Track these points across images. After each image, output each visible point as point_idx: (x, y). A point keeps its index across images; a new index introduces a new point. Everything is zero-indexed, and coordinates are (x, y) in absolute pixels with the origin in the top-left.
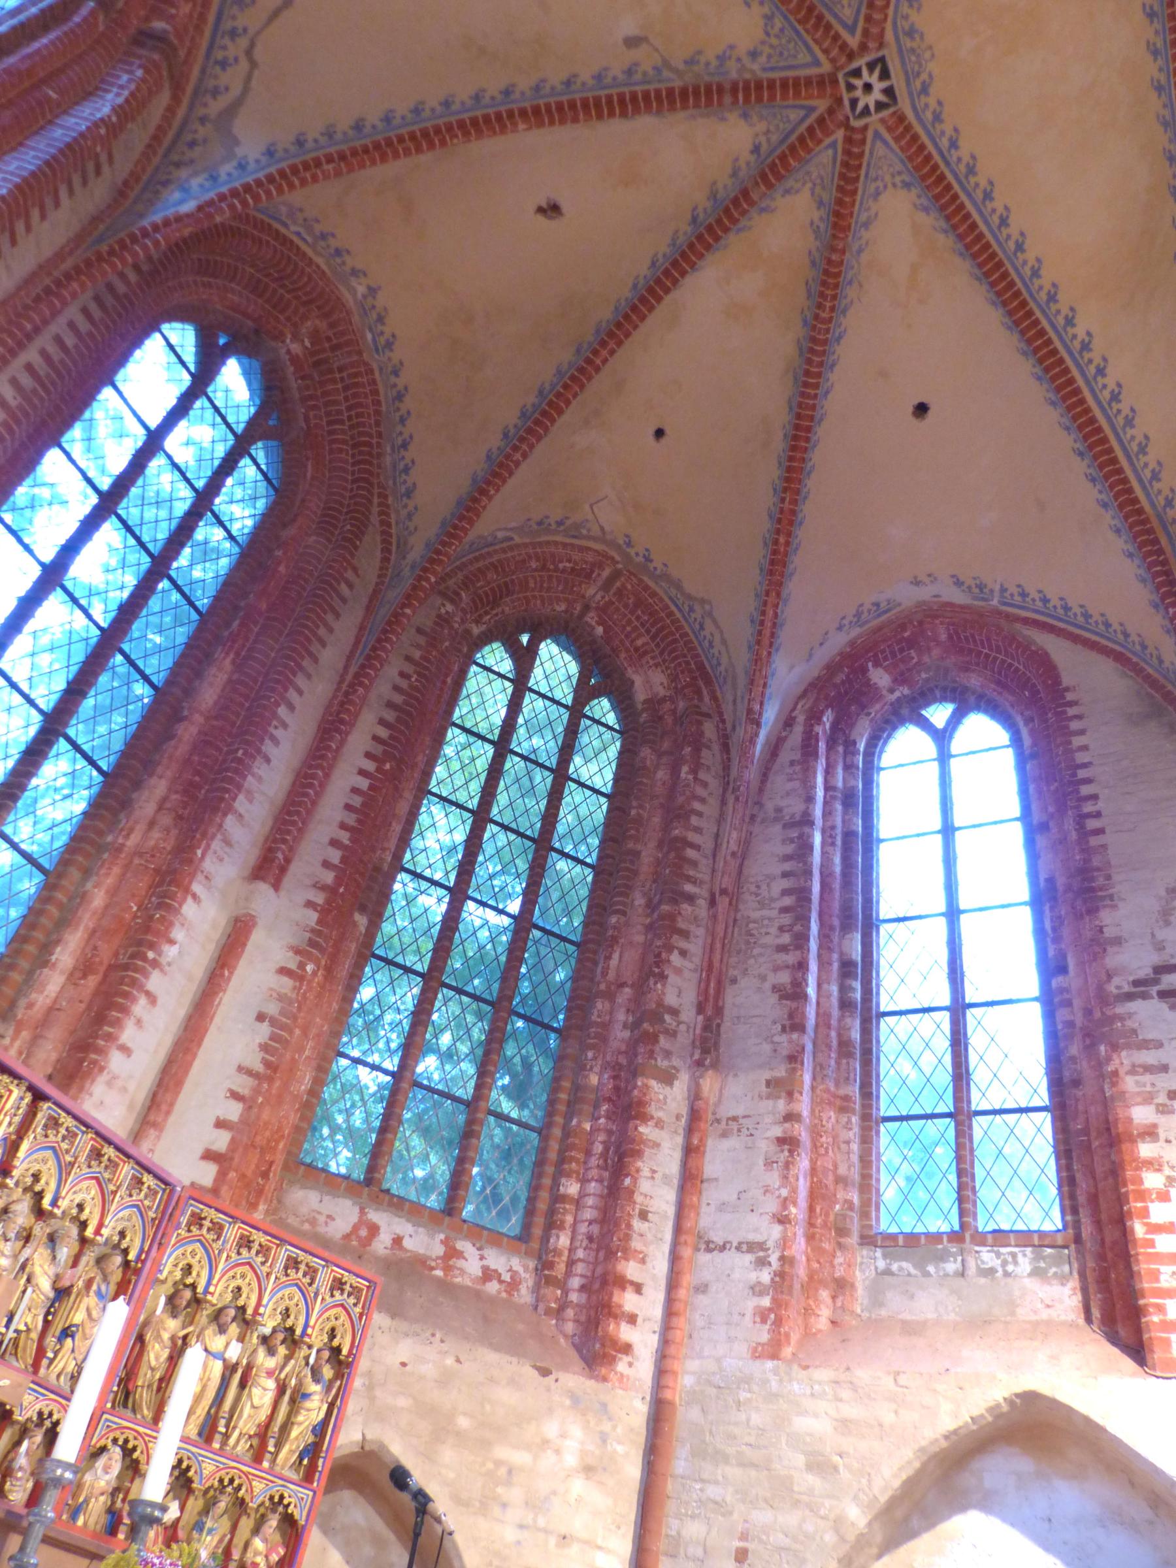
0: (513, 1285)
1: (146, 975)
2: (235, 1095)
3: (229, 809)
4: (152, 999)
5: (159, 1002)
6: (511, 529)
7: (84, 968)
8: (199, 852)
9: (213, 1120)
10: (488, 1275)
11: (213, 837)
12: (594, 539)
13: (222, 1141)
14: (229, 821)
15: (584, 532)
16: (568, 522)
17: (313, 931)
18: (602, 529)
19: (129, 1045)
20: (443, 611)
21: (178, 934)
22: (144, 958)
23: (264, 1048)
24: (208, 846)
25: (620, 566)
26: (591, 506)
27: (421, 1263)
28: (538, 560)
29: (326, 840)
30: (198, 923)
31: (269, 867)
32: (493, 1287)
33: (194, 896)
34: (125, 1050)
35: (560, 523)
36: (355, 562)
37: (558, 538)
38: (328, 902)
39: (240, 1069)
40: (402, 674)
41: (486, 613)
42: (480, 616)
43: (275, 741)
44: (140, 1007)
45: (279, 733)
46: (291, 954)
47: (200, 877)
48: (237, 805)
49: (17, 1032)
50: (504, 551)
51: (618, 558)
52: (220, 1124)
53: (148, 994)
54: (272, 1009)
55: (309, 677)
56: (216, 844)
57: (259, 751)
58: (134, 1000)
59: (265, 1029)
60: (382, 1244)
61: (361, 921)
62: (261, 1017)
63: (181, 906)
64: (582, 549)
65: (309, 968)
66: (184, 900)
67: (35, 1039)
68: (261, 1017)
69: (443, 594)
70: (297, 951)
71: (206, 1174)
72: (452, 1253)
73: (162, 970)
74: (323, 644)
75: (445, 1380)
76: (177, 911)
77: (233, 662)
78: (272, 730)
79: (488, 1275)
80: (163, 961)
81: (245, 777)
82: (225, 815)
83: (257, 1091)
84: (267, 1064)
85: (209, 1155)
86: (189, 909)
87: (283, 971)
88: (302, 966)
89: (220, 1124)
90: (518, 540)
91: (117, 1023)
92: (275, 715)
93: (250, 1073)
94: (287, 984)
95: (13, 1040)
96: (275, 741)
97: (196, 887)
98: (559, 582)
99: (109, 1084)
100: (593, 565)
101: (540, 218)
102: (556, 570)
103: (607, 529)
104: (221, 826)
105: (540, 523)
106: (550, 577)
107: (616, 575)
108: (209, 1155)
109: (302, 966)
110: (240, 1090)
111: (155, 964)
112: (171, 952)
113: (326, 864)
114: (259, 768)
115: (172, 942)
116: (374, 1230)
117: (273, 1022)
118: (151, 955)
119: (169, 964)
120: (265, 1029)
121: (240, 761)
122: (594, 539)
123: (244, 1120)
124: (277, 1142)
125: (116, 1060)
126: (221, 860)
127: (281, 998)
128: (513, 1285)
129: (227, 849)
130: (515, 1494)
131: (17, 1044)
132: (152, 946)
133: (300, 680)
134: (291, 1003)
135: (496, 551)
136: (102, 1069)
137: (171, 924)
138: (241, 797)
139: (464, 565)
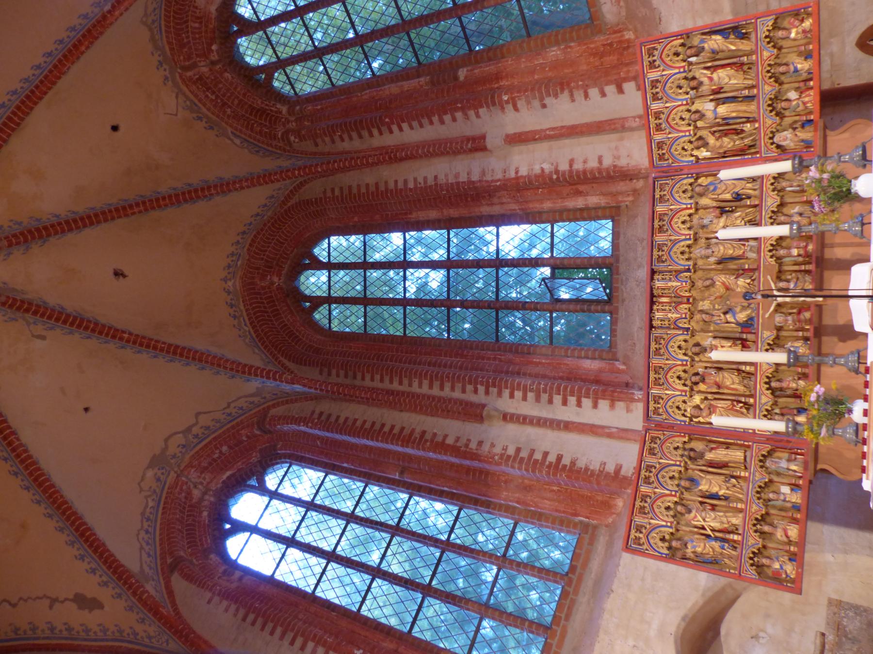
1: (564, 173)
2: (586, 96)
4: (571, 162)
5: (570, 157)
6: (229, 139)
7: (579, 193)
8: (498, 184)
9: (604, 99)
11: (487, 181)
12: (184, 94)
13: (610, 89)
14: (475, 178)
15: (188, 103)
16: (195, 115)
17: (488, 107)
18: (177, 97)
19: (597, 160)
20: (297, 140)
21: (537, 170)
22: (558, 178)
23: (556, 96)
24: (492, 181)
25: (179, 70)
26: (176, 115)
28: (225, 112)
29: (443, 127)
30: (527, 162)
31: (477, 145)
33: (517, 173)
34: (600, 159)
35: (200, 119)
36: (322, 196)
37: (204, 110)
38: (469, 108)
39: (573, 101)
41: (271, 110)
42: (276, 112)
43: (425, 179)
44: (578, 166)
45: (420, 180)
46: (506, 110)
47: (507, 176)
48: (466, 180)
49: (622, 202)
50: (241, 131)
51: (177, 75)
52: (603, 94)
53: (571, 166)
54: (536, 103)
55: (386, 183)
56: (488, 178)
57: (436, 184)
58: (578, 171)
59: (547, 101)
61: (462, 74)
62: (544, 106)
63: (525, 177)
64: (196, 96)
65: (505, 98)
66: (522, 176)
67: (621, 193)
68: (544, 106)
70: (503, 108)
71: (629, 87)
73: (557, 166)
74: (367, 185)
76: (529, 176)
77: (411, 213)
78: (422, 185)
80: (553, 168)
81: (452, 184)
82: (474, 182)
83: (578, 87)
84: (562, 90)
86: (523, 172)
87: (516, 109)
88: (507, 102)
89: (603, 94)
90: (229, 130)
91: (592, 171)
92: (416, 188)
93: (572, 95)
94: (520, 104)
95: (625, 201)
96: (425, 179)
97: (513, 175)
98: (220, 89)
99: (618, 158)
100: (194, 83)
101: (126, 273)
102: (217, 97)
103: (174, 95)
104: (480, 181)
105: (211, 128)
106: (224, 95)
107: (186, 69)
109: (507, 102)
110: (583, 95)
111: (557, 172)
112: (547, 167)
113: (454, 119)
114: (442, 179)
115: (543, 170)
117: (542, 99)
118: (555, 177)
119: (552, 164)
120: (547, 101)
121: (447, 190)
122: (184, 94)
123: (595, 85)
124: (592, 49)
125: (607, 162)
126: (493, 170)
127: (528, 103)
129: (486, 170)
131: (625, 199)
132: (551, 179)
133: (391, 185)
134: (527, 97)
135: (245, 134)
136: (615, 166)
137: (536, 176)
138: (461, 180)
139: (268, 145)
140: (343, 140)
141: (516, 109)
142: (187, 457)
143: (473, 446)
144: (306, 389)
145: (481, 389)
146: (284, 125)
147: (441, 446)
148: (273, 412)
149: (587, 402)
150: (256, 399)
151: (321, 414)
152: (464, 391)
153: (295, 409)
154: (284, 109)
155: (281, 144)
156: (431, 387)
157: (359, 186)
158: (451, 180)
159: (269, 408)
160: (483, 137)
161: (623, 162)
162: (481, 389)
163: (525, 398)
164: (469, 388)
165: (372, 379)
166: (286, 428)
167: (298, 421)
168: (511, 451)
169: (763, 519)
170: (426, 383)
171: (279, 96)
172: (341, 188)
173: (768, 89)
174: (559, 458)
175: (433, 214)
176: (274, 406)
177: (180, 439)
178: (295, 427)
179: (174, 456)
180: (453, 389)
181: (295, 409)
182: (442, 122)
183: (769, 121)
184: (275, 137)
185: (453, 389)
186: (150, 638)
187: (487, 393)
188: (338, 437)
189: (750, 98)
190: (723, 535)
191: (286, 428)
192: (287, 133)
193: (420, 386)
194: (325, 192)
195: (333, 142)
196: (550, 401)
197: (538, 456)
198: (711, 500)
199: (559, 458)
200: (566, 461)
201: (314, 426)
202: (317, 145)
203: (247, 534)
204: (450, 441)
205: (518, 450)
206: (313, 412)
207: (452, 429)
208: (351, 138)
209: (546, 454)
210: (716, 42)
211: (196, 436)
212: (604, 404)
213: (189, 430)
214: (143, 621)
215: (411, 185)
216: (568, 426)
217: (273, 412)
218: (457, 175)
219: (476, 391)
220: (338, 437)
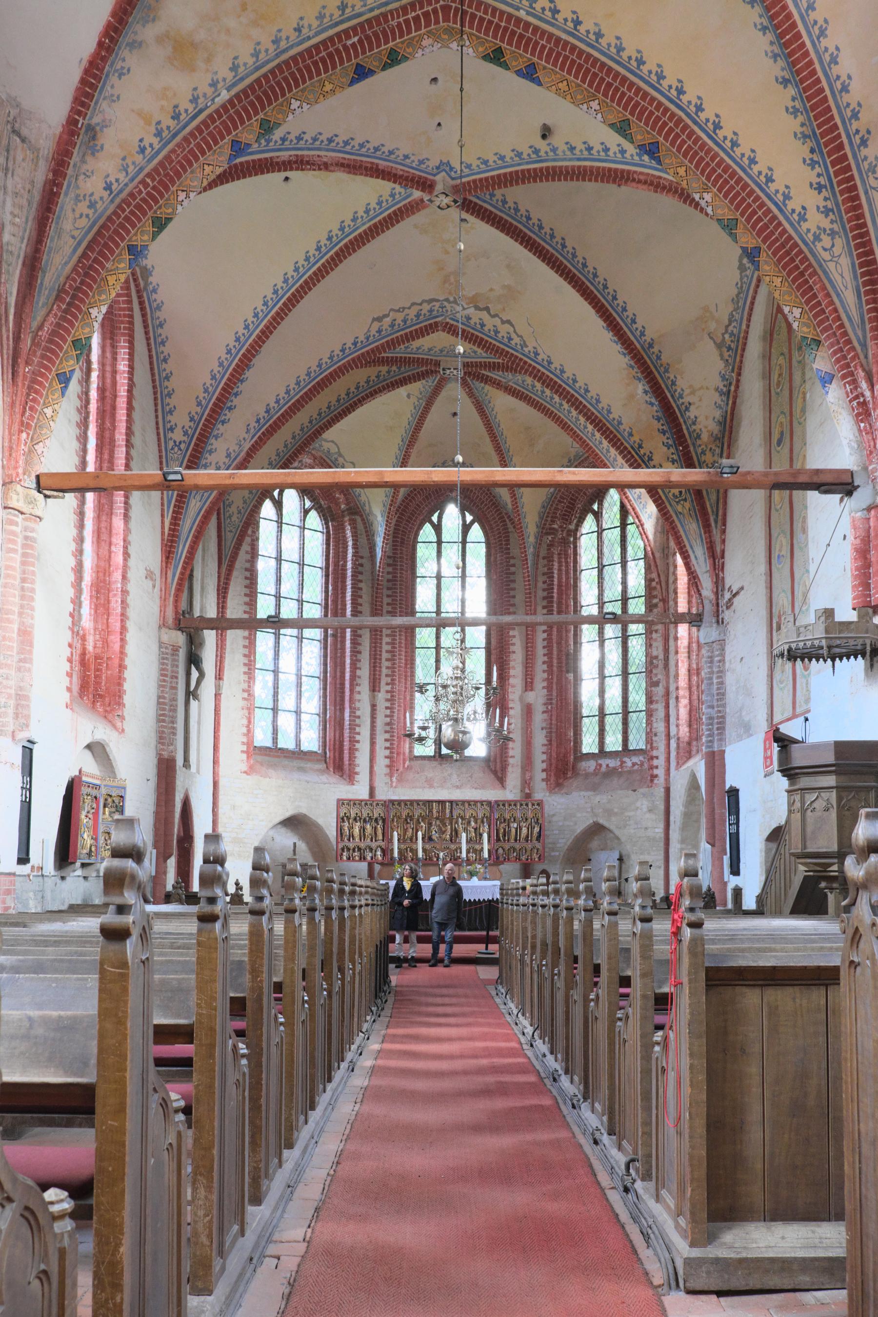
0: (642, 764)
3: (509, 677)
10: (634, 764)
27: (615, 769)
32: (636, 767)
34: (513, 757)
40: (544, 582)
43: (514, 644)
45: (514, 640)
54: (544, 725)
59: (544, 731)
60: (604, 769)
69: (547, 534)
72: (622, 762)
74: (514, 597)
75: (609, 801)
79: (634, 764)
85: (543, 771)
87: (544, 712)
96: (514, 644)
108: (543, 771)
113: (544, 671)
114: (513, 657)
116: (601, 765)
120: (544, 731)
125: (511, 761)
128: (642, 764)
130: (632, 822)
140: (544, 582)
141: (544, 712)
142: (320, 454)
143: (358, 689)
144: (378, 560)
145: (389, 688)
146: (561, 527)
147: (354, 667)
148: (359, 519)
149: (387, 752)
150: (367, 508)
151: (361, 565)
152: (387, 676)
153: (363, 540)
154: (572, 527)
155: (547, 526)
156: (387, 652)
157: (514, 589)
158: (512, 664)
159: (361, 516)
160: (532, 690)
161: (510, 769)
162: (389, 688)
163: (386, 716)
164: (389, 680)
165: (388, 604)
166: (349, 533)
167: (355, 546)
168: (358, 713)
169: (360, 849)
170: (389, 647)
171: (581, 520)
172: (514, 573)
173: (517, 846)
174: (358, 742)
175: (494, 642)
176: (363, 520)
177: (334, 449)
178: (350, 543)
179: (321, 446)
180: (387, 668)
181: (363, 540)
182: (544, 663)
183: (507, 846)
184: (553, 522)
185: (387, 668)
186: (230, 517)
187: (387, 692)
188: (349, 582)
189: (516, 840)
190: (351, 836)
191: (349, 533)
192: (553, 531)
193: (387, 643)
194: (513, 558)
195: (544, 574)
196: (386, 732)
197: (358, 729)
198: (363, 829)
199: (358, 742)
200: (357, 746)
201: (354, 563)
202: (544, 558)
203: (275, 518)
204: (358, 672)
205: (359, 717)
206: (362, 557)
207: (364, 672)
208: (544, 590)
209: (359, 734)
210: (537, 829)
211: (336, 459)
212: (387, 761)
213: (340, 455)
214: (239, 512)
215: (511, 633)
216: (373, 743)
217: (359, 519)
218: (514, 668)
219: (387, 684)
220: (349, 582)
